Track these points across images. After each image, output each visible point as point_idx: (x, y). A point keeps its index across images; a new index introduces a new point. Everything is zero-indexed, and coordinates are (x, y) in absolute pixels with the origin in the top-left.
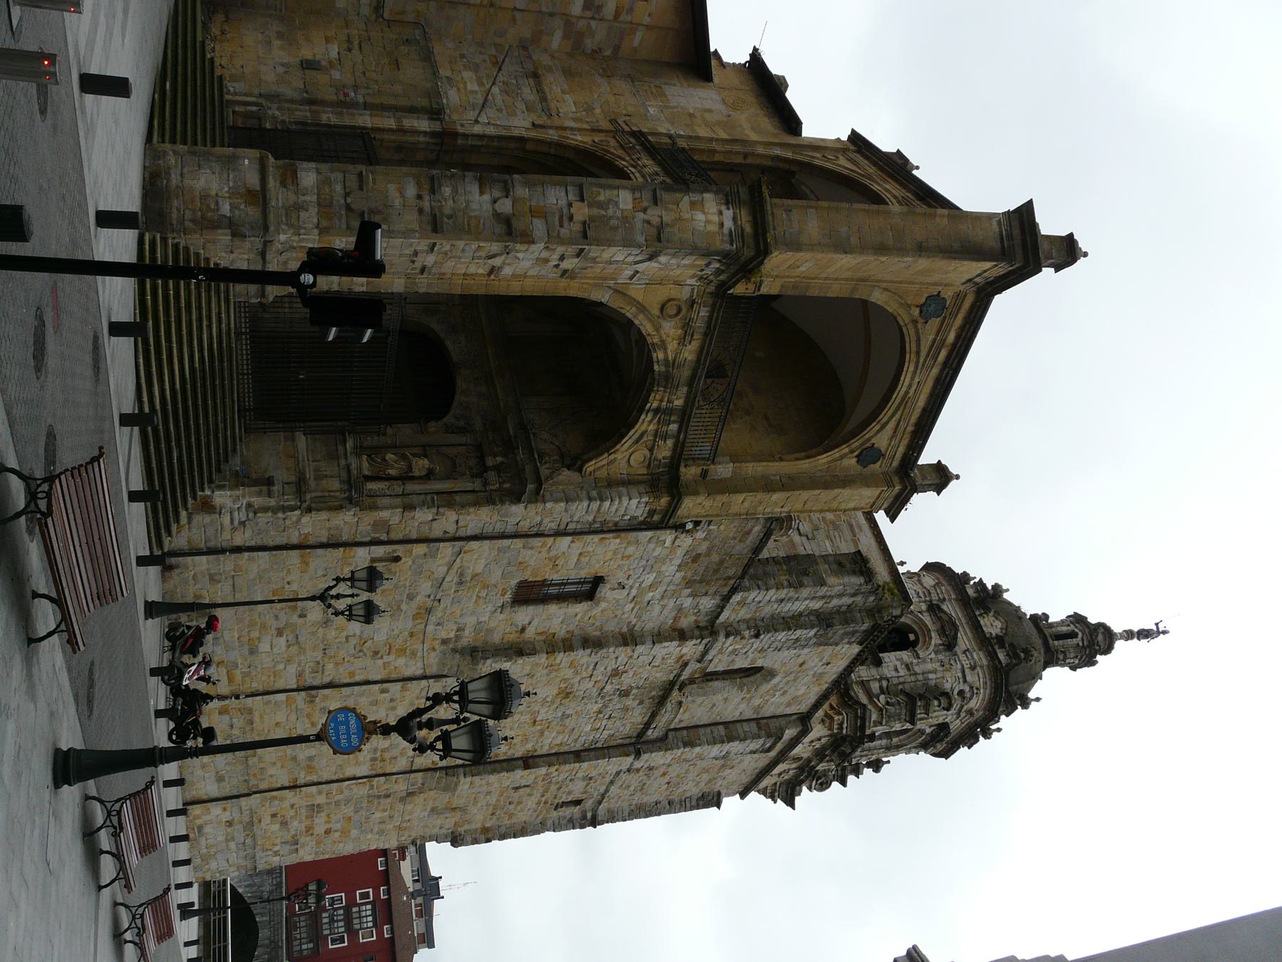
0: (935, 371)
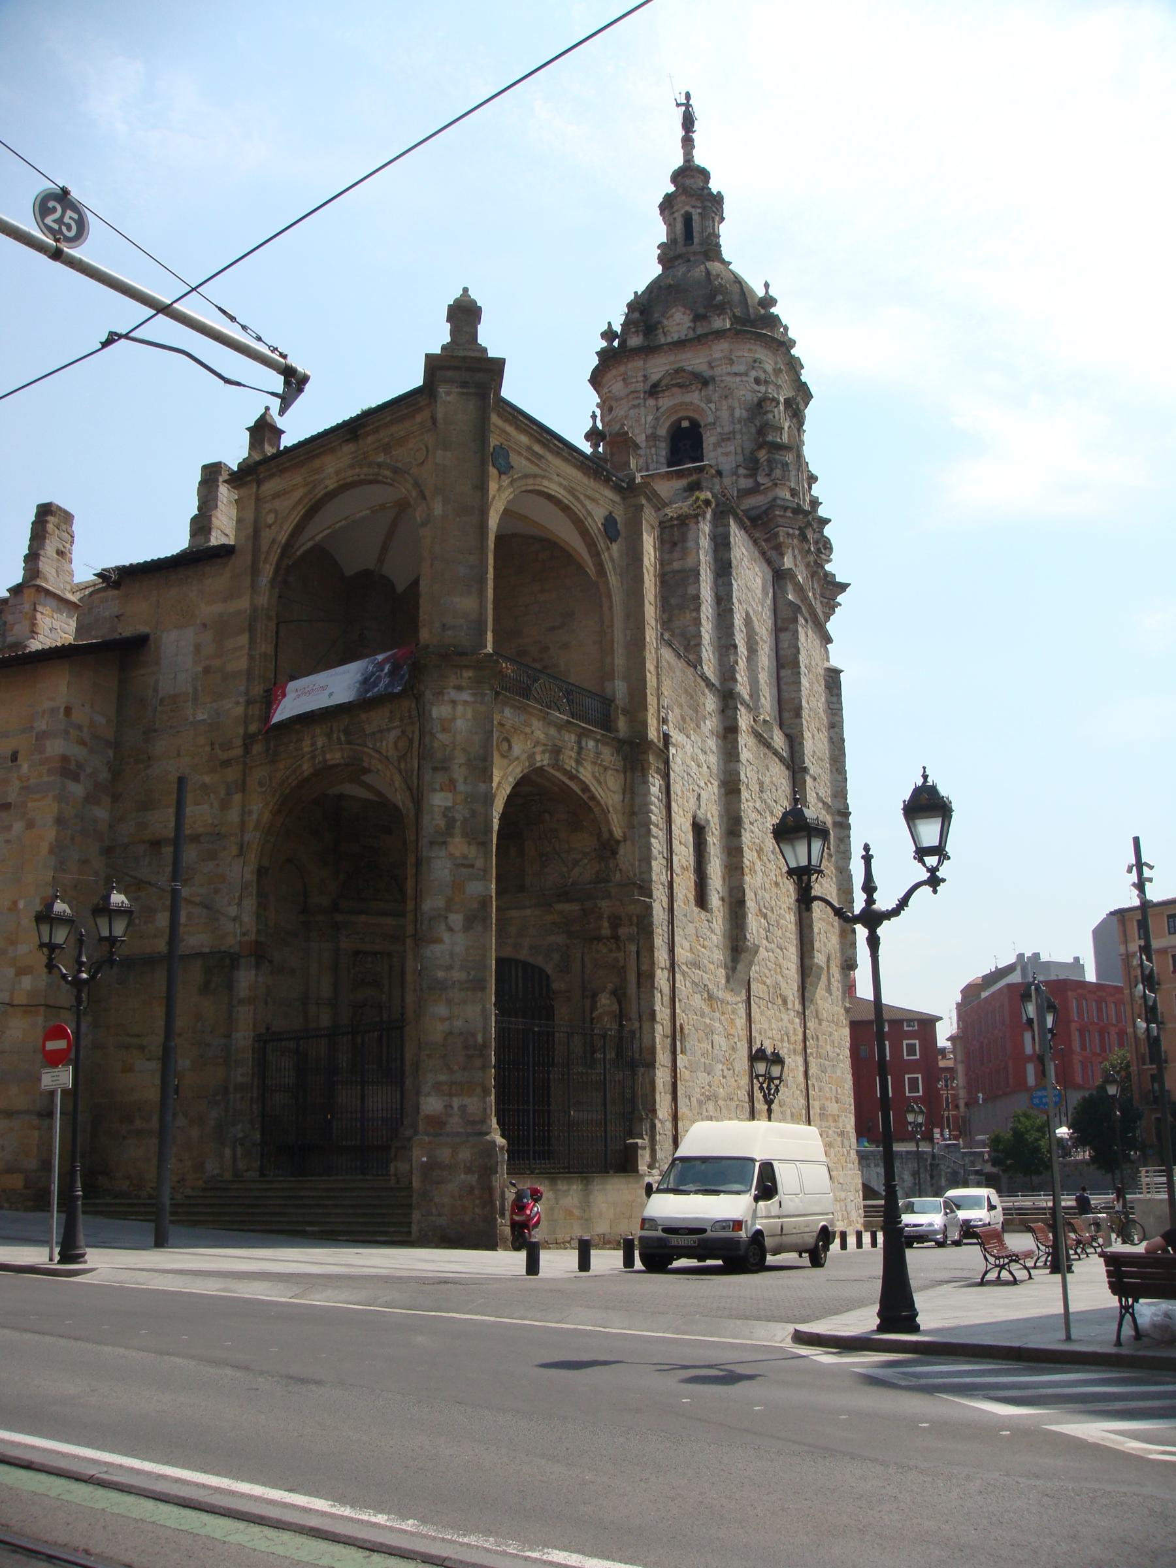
0: (550, 457)
